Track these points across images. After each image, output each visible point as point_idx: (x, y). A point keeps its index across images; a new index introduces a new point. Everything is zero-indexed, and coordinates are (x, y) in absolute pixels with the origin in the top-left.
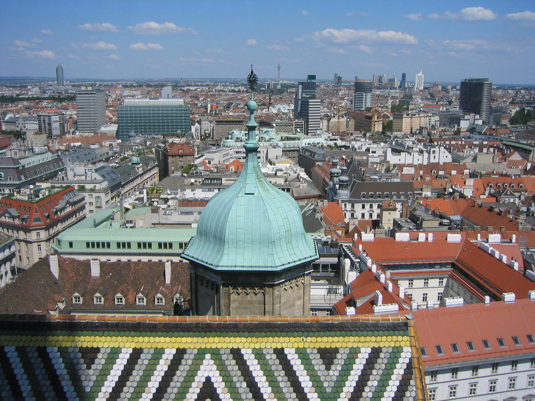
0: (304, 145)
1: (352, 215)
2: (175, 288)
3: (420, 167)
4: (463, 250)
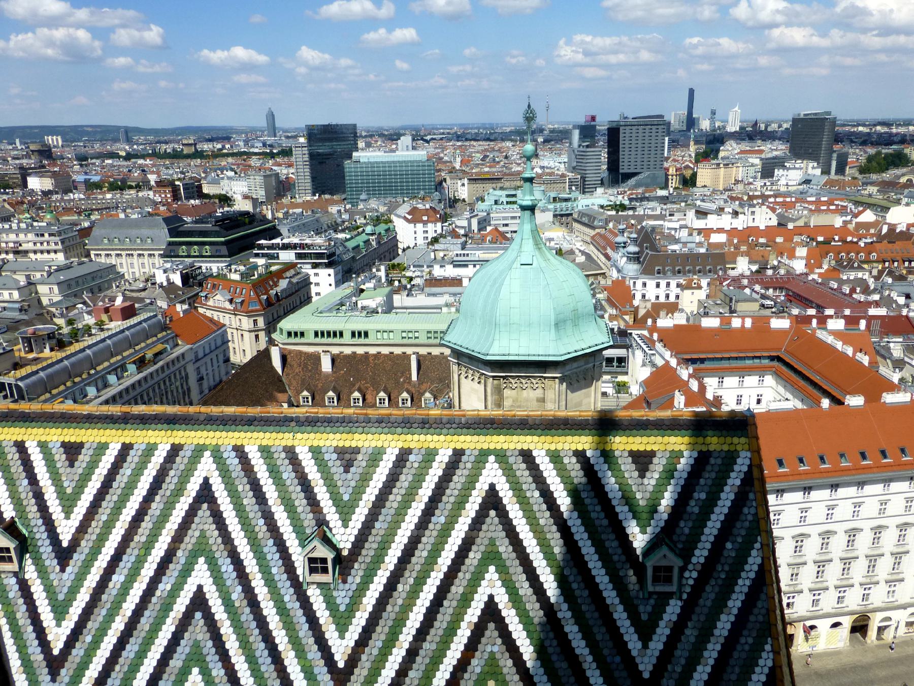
0: (580, 208)
1: (644, 296)
2: (423, 387)
3: (732, 233)
4: (792, 340)
